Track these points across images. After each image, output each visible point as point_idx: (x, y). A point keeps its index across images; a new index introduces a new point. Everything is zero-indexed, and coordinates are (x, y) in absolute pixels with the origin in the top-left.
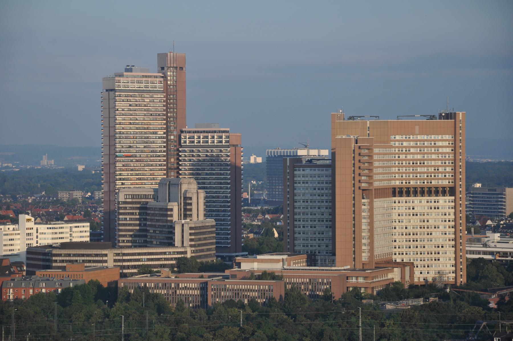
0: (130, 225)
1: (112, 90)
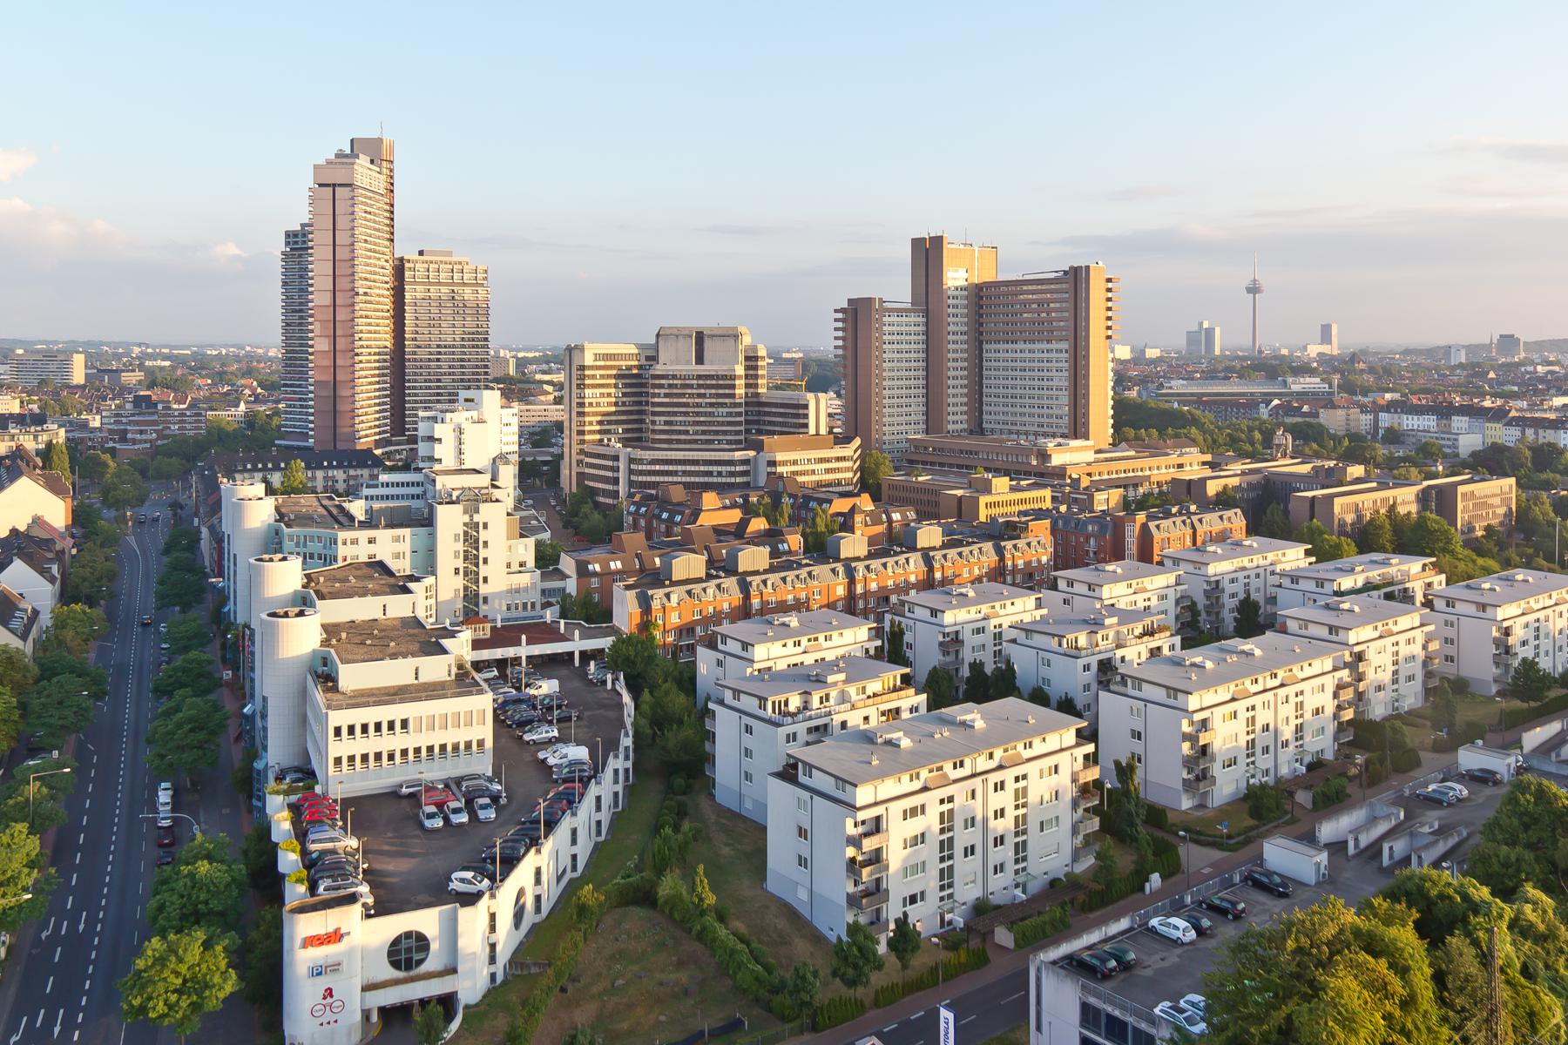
0: (598, 404)
1: (340, 185)
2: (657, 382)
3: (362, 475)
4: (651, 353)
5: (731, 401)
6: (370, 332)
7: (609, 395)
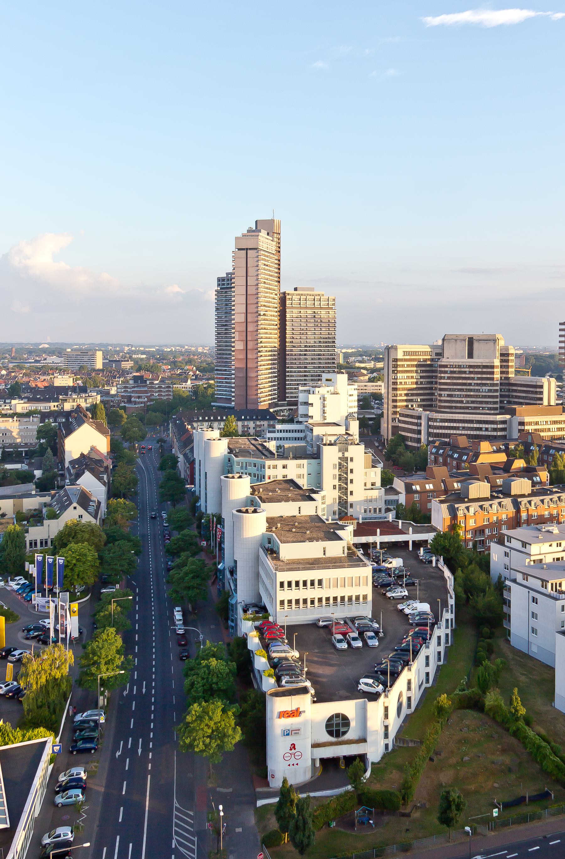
0: (405, 383)
1: (250, 249)
2: (443, 369)
3: (264, 425)
4: (439, 351)
5: (491, 382)
6: (266, 338)
7: (412, 377)
